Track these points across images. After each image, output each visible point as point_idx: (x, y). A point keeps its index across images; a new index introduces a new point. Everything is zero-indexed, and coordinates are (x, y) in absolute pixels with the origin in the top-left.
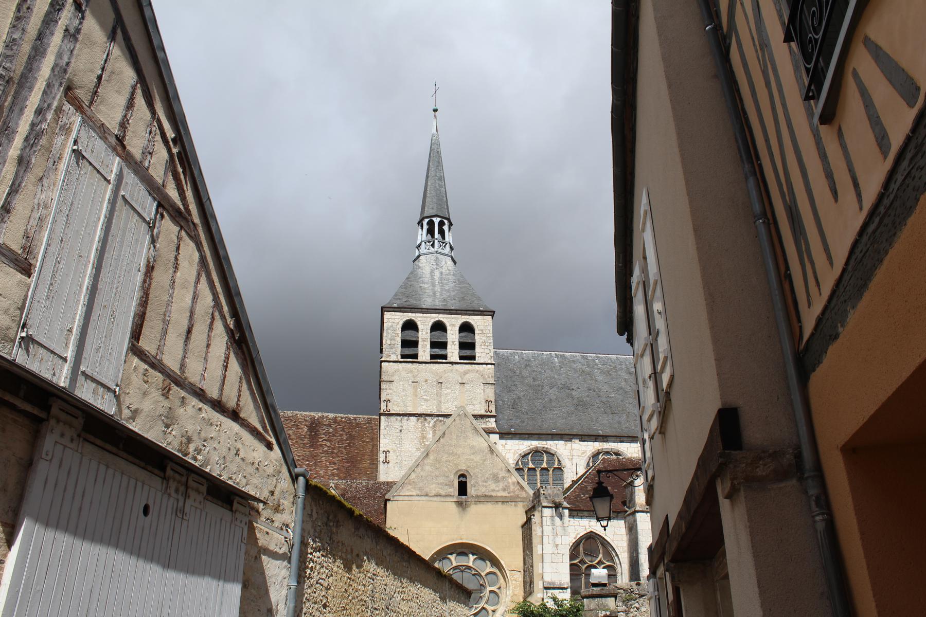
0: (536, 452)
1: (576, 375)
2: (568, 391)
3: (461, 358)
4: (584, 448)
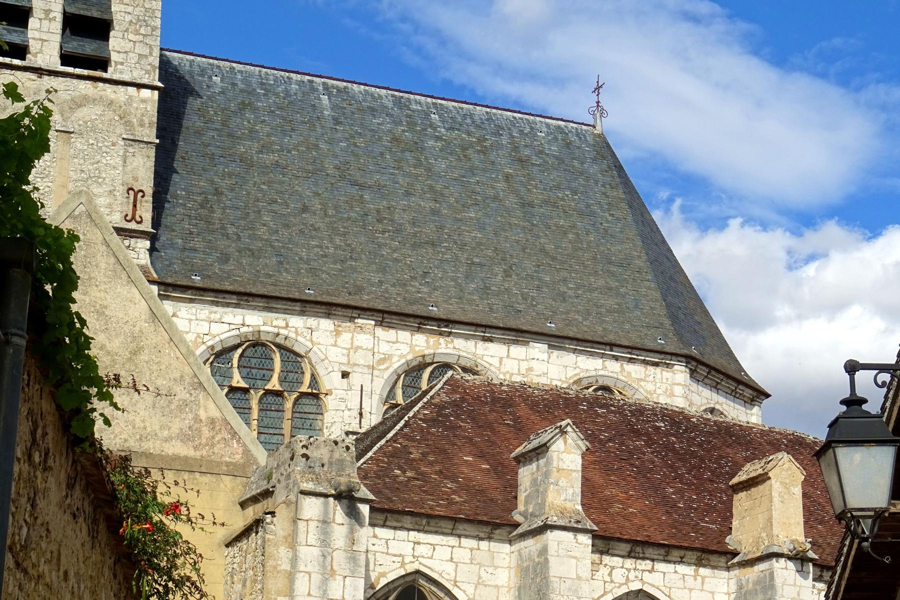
0: (256, 348)
1: (377, 150)
2: (354, 191)
3: (67, 59)
4: (384, 348)
